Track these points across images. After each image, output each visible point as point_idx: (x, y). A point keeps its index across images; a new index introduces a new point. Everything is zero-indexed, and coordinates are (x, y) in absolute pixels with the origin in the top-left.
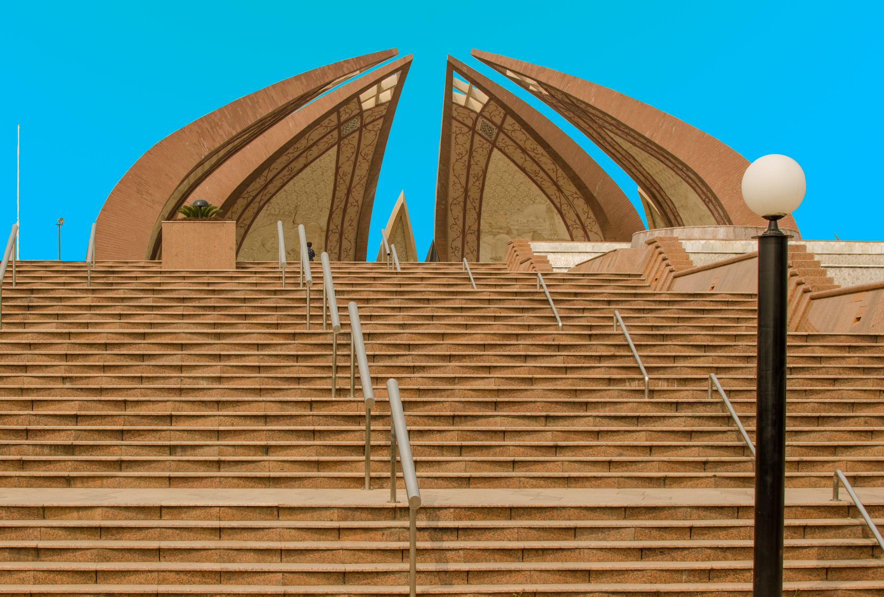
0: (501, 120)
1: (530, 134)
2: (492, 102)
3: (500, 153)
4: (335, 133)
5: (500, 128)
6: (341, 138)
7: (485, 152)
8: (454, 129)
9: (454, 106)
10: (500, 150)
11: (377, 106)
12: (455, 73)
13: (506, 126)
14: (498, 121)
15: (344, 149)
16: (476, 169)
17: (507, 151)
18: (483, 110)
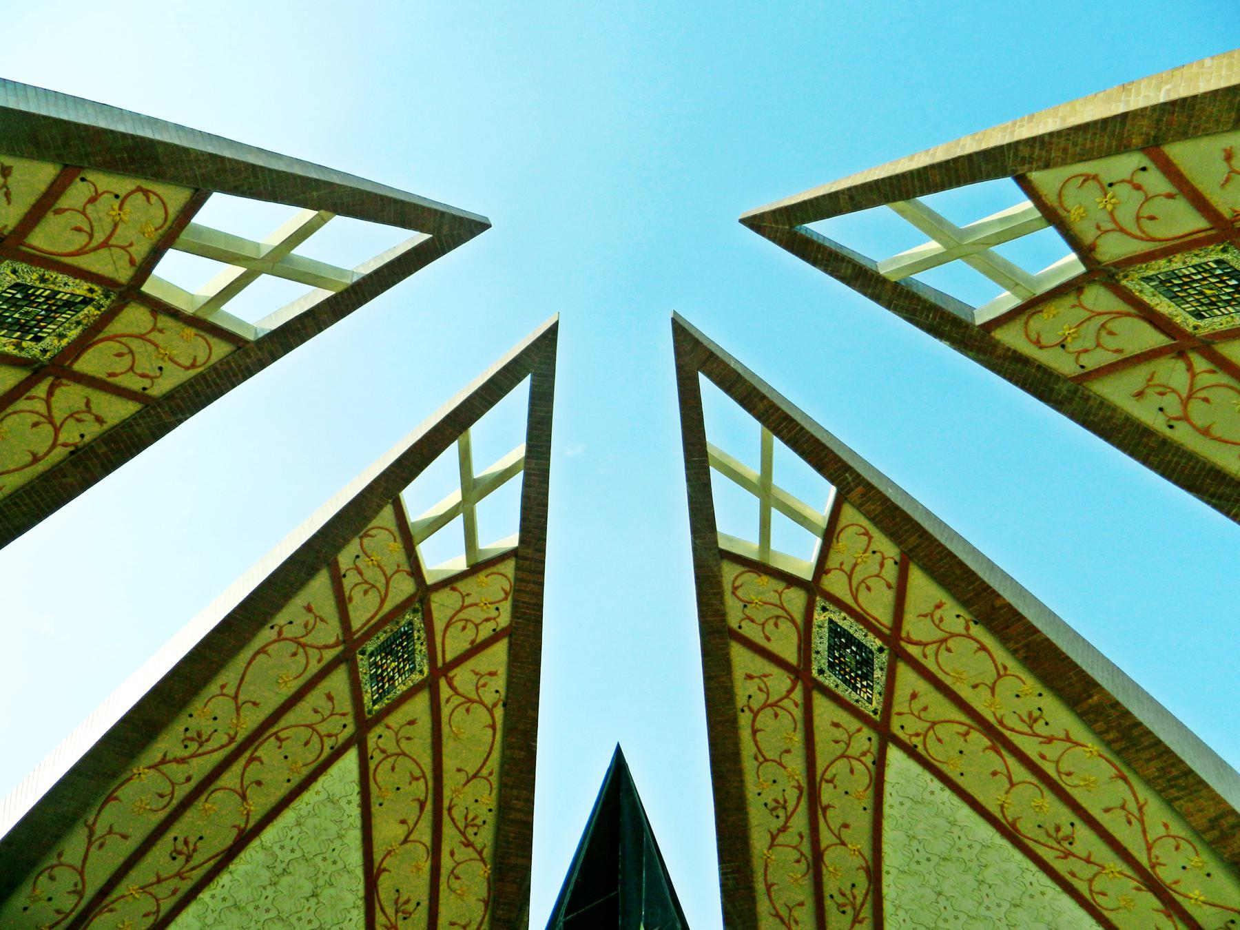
0: (889, 597)
1: (1004, 639)
2: (849, 514)
3: (914, 767)
4: (338, 681)
5: (894, 639)
6: (365, 724)
7: (862, 778)
8: (743, 690)
9: (729, 572)
10: (911, 751)
11: (478, 567)
12: (703, 380)
13: (914, 627)
14: (879, 606)
15: (382, 776)
16: (843, 868)
17: (935, 752)
18: (821, 567)
